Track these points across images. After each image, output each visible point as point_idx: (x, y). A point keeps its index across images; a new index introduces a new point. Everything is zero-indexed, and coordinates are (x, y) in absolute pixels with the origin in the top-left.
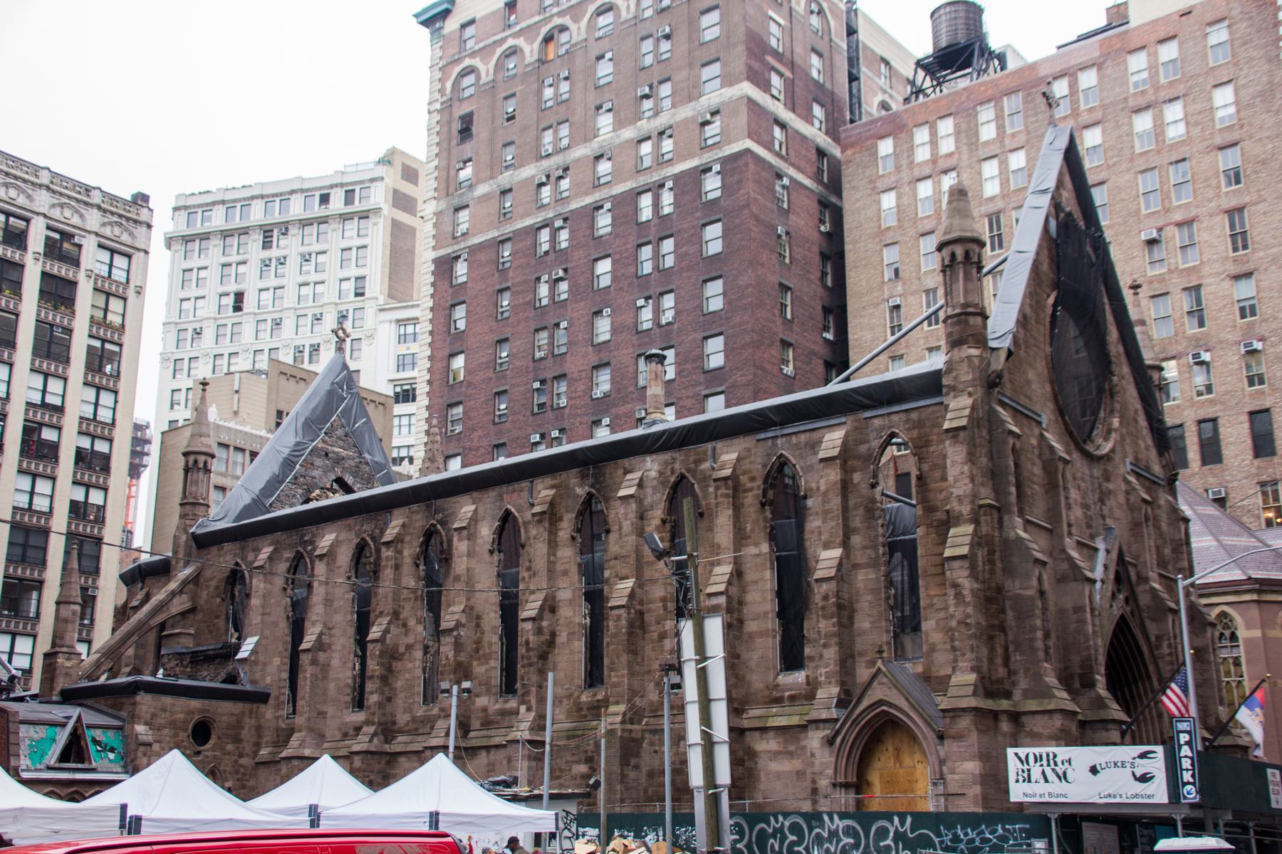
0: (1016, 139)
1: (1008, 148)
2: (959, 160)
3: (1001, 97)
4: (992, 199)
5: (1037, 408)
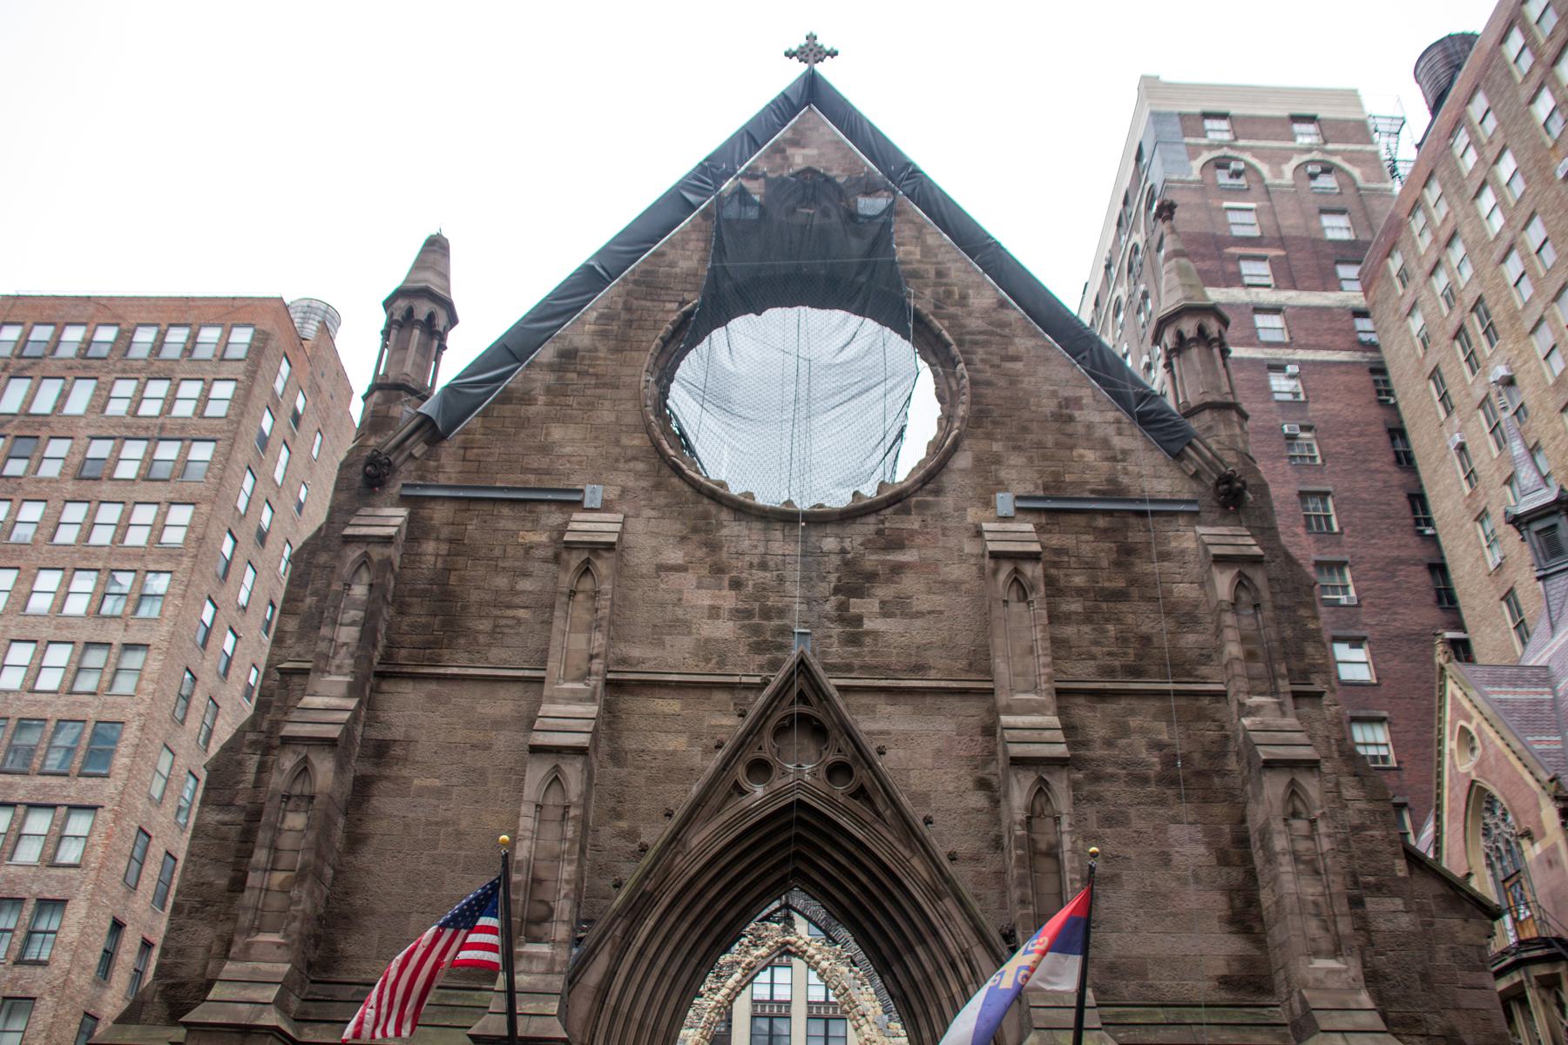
0: (1496, 142)
1: (1492, 161)
2: (1456, 216)
3: (1465, 111)
4: (1498, 236)
5: (575, 481)
